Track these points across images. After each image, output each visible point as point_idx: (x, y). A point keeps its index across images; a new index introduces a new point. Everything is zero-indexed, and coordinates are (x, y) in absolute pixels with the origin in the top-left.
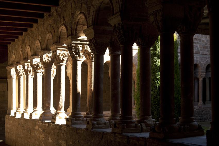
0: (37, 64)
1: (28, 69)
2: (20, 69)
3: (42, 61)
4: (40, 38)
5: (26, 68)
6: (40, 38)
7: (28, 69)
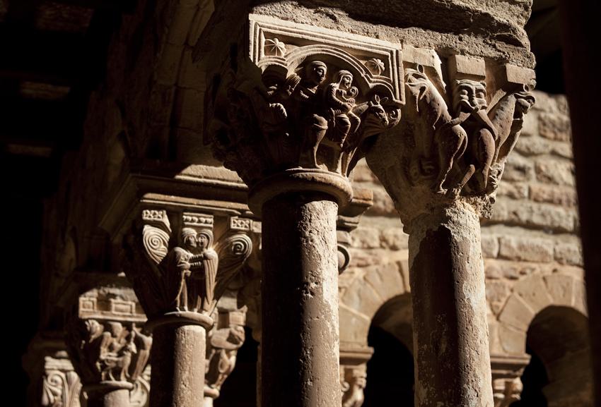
0: (307, 66)
1: (172, 258)
7: (172, 258)
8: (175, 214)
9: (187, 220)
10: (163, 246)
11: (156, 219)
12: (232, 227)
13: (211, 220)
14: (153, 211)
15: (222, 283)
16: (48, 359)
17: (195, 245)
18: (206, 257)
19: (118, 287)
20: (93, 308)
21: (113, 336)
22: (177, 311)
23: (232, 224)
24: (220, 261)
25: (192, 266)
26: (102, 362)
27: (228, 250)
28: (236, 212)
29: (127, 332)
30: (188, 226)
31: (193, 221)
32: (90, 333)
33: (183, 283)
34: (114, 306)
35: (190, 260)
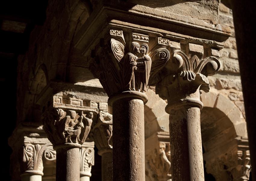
1: (127, 59)
7: (126, 60)
8: (128, 33)
9: (134, 37)
10: (121, 52)
11: (117, 35)
12: (159, 43)
13: (147, 38)
14: (115, 31)
15: (153, 76)
16: (26, 137)
17: (139, 52)
18: (145, 59)
19: (74, 91)
20: (61, 102)
21: (72, 118)
22: (130, 90)
23: (159, 42)
24: (152, 63)
25: (138, 64)
26: (66, 132)
27: (157, 56)
28: (161, 34)
29: (79, 116)
30: (135, 41)
31: (137, 38)
32: (59, 116)
33: (133, 73)
34: (72, 101)
35: (137, 60)
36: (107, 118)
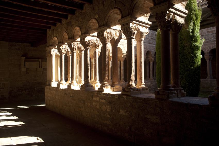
0: (88, 41)
1: (74, 47)
2: (63, 48)
3: (102, 37)
4: (98, 16)
5: (72, 46)
6: (97, 16)
7: (74, 47)
36: (69, 50)
